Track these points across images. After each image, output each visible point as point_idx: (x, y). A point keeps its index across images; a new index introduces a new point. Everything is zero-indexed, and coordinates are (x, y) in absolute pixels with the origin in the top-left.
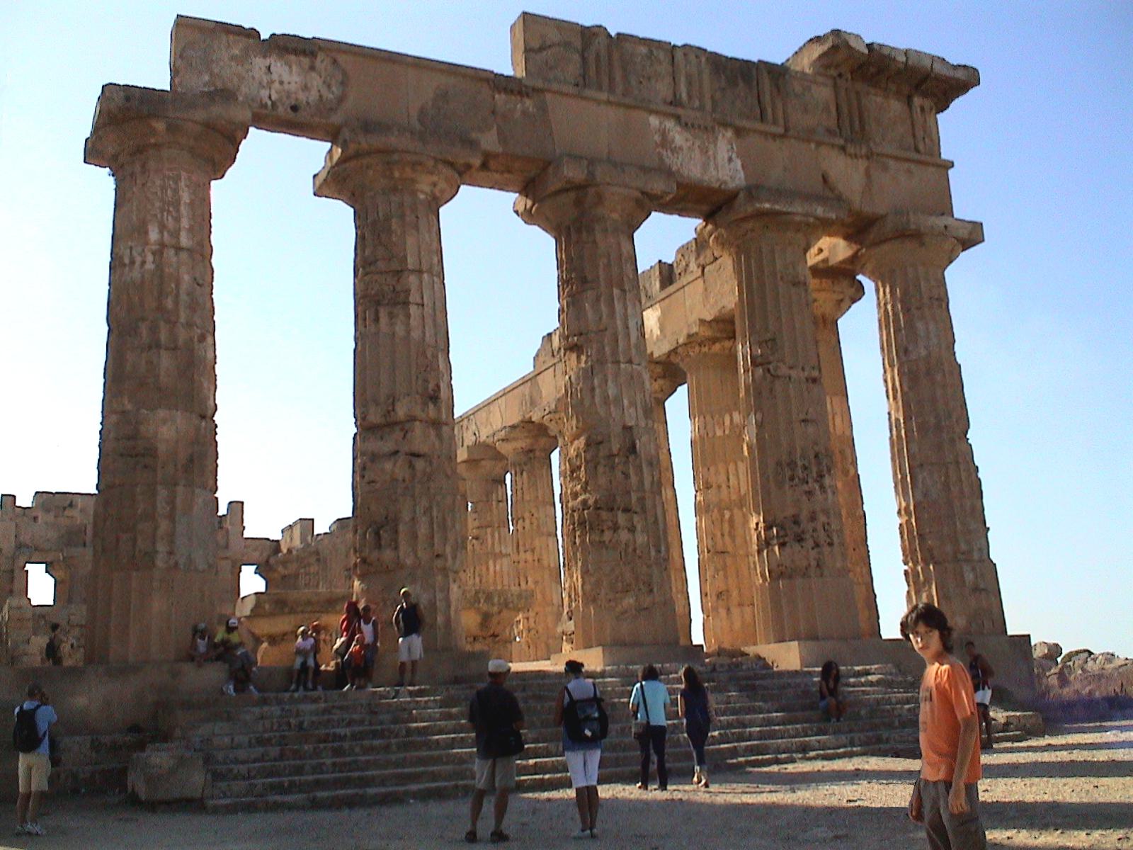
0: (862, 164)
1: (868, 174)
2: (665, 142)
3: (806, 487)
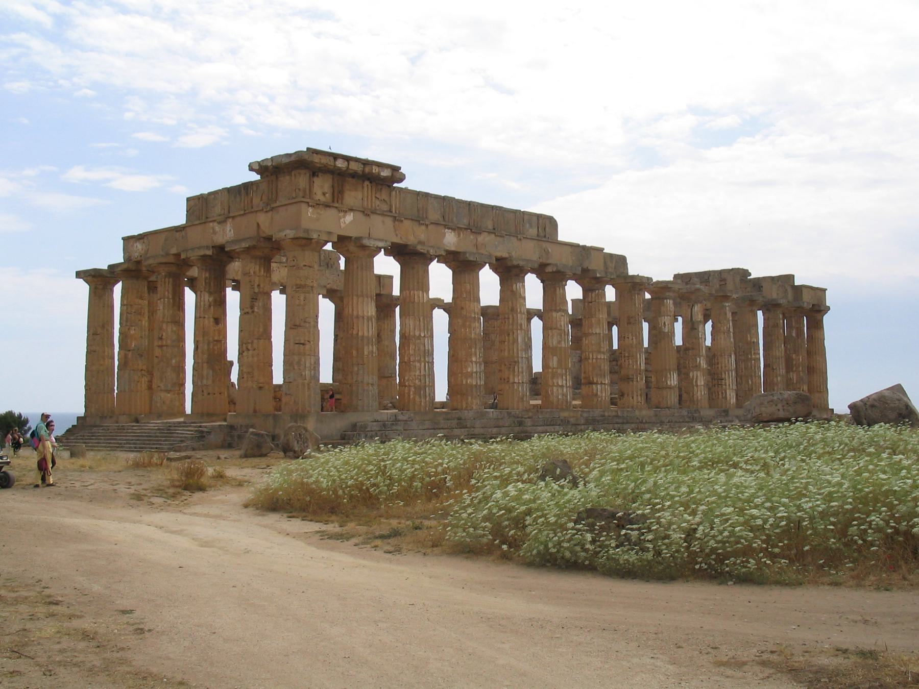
2: (214, 233)
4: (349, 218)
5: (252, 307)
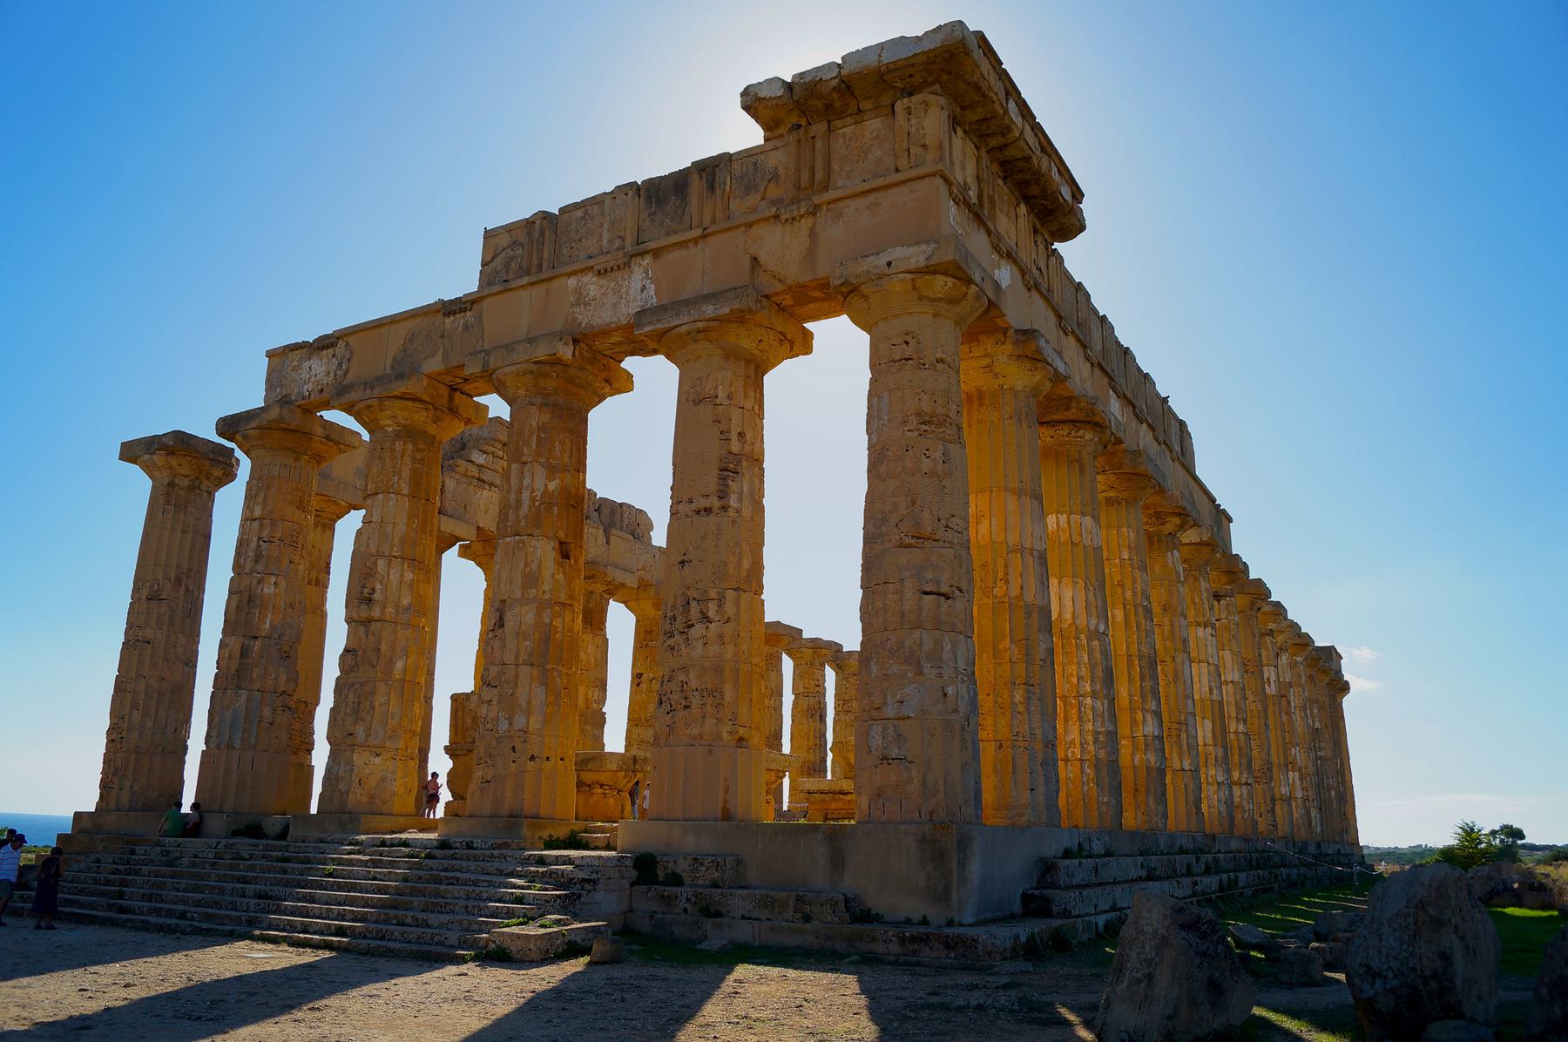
0: (806, 224)
1: (813, 234)
2: (581, 299)
3: (671, 642)
5: (723, 495)
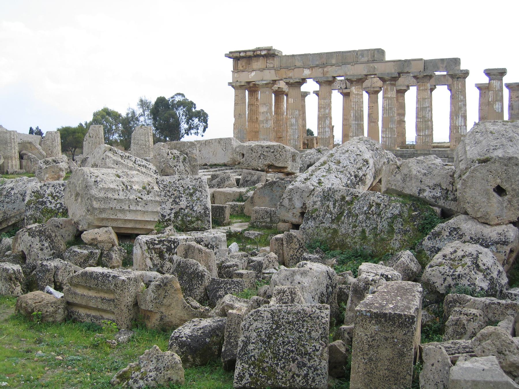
4: (253, 74)
